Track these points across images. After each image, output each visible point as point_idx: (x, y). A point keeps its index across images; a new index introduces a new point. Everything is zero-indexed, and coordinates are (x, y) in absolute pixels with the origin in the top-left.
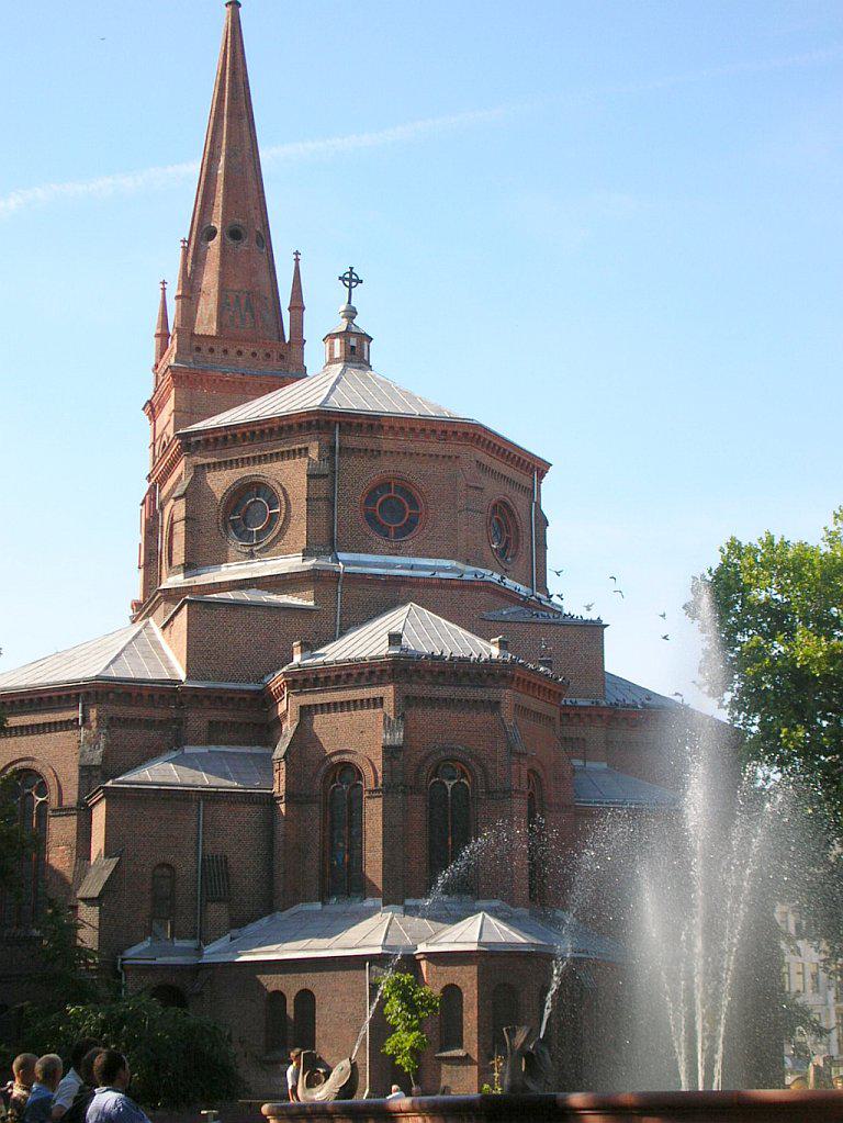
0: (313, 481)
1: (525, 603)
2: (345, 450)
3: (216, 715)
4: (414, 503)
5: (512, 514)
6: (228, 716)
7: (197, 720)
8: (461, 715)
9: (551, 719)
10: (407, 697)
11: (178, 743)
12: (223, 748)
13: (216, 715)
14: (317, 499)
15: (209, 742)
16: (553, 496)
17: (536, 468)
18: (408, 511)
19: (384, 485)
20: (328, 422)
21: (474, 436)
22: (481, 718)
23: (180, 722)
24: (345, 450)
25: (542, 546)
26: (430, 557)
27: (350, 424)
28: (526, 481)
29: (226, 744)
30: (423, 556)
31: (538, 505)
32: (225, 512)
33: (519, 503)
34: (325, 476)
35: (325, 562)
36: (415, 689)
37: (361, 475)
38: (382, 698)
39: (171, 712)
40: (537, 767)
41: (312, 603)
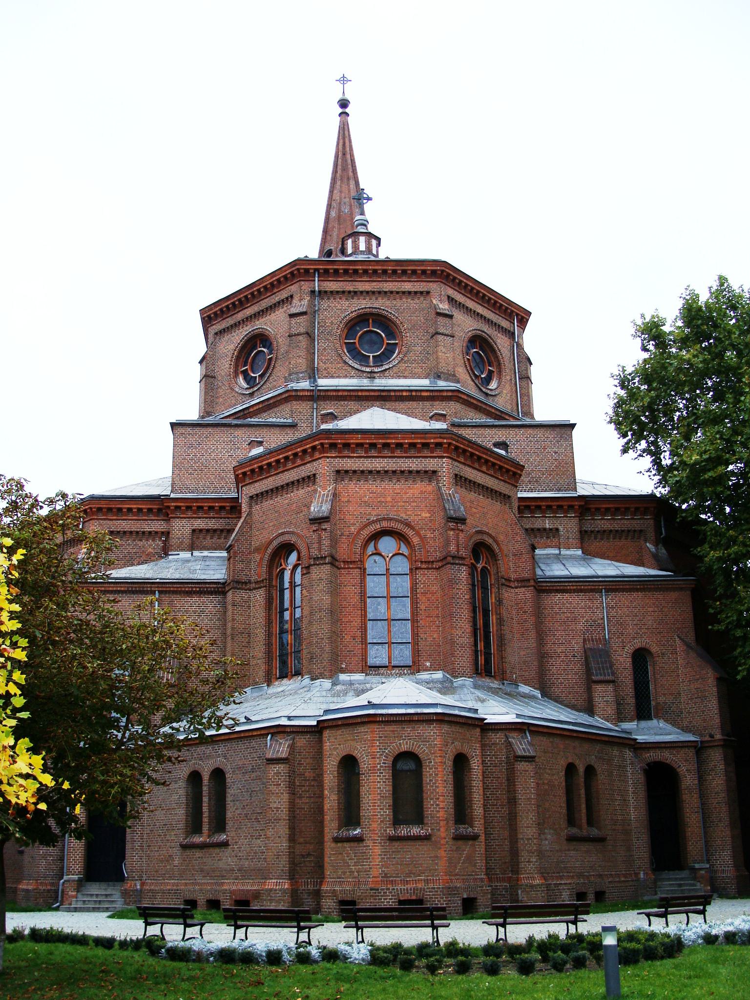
0: (293, 321)
1: (499, 415)
2: (323, 294)
3: (200, 524)
4: (391, 334)
5: (493, 351)
6: (212, 524)
7: (181, 527)
8: (397, 486)
9: (505, 498)
10: (338, 472)
11: (165, 552)
12: (206, 553)
13: (200, 524)
14: (298, 335)
15: (192, 548)
16: (532, 339)
17: (522, 317)
18: (386, 341)
19: (362, 319)
20: (307, 271)
21: (442, 273)
22: (419, 487)
23: (167, 534)
24: (323, 294)
25: (526, 378)
26: (405, 377)
27: (326, 271)
28: (505, 324)
29: (208, 550)
30: (399, 377)
31: (520, 347)
32: (236, 366)
33: (501, 342)
34: (304, 313)
35: (305, 385)
36: (349, 464)
37: (337, 312)
38: (314, 475)
39: (157, 525)
40: (490, 541)
41: (290, 421)
